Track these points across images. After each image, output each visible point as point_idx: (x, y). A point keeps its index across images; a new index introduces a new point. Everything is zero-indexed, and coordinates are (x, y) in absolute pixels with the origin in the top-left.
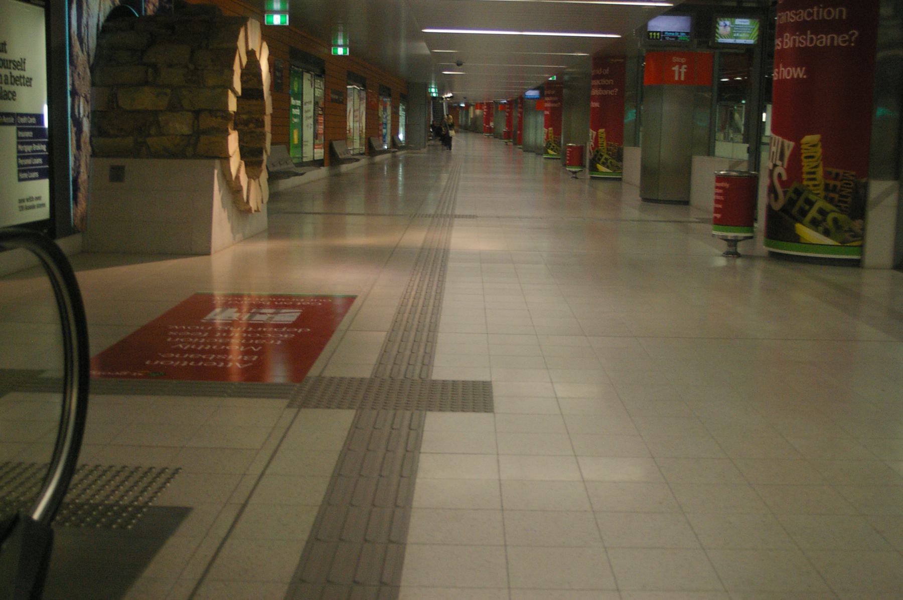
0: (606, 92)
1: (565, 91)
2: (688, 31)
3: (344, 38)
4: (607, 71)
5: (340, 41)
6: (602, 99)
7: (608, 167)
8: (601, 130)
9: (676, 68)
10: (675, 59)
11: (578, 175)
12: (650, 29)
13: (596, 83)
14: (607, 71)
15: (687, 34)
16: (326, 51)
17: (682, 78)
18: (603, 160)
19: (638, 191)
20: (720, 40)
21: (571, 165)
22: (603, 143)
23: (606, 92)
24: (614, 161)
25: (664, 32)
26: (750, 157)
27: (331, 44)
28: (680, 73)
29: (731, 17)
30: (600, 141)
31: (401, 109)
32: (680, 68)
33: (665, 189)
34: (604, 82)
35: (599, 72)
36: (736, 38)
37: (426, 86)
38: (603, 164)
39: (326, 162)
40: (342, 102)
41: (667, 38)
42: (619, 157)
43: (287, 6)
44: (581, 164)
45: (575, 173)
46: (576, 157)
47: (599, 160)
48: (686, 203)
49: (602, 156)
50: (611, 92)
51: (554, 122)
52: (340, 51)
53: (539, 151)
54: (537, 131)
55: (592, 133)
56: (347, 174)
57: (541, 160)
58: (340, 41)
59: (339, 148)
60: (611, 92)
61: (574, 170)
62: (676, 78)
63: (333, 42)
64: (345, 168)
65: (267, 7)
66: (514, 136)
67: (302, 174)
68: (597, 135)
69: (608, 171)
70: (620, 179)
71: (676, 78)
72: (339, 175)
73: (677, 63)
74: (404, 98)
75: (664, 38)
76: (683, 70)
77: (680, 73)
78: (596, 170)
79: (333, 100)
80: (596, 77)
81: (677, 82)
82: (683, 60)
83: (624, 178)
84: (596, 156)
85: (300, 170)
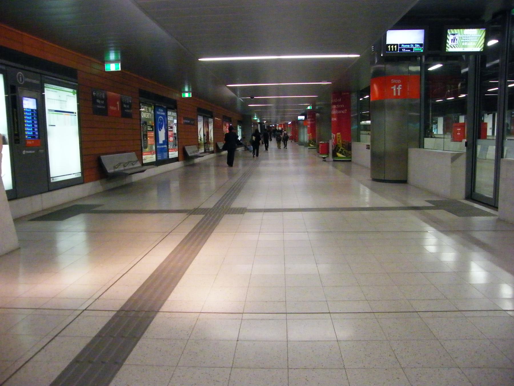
0: (340, 112)
1: (317, 115)
2: (423, 43)
3: (189, 88)
4: (340, 100)
5: (186, 89)
6: (338, 116)
7: (343, 154)
8: (339, 134)
9: (394, 88)
10: (393, 81)
11: (326, 159)
12: (388, 42)
13: (334, 107)
14: (340, 100)
15: (421, 45)
16: (178, 95)
17: (399, 94)
18: (340, 150)
19: (369, 171)
20: (450, 49)
21: (322, 154)
22: (340, 141)
23: (340, 112)
24: (346, 151)
25: (400, 45)
26: (468, 149)
27: (182, 91)
28: (397, 90)
29: (460, 28)
30: (338, 140)
31: (238, 127)
32: (397, 87)
33: (391, 171)
34: (338, 106)
35: (335, 101)
36: (464, 47)
37: (251, 116)
38: (340, 153)
39: (180, 159)
40: (193, 125)
41: (404, 50)
42: (349, 148)
43: (119, 57)
44: (327, 153)
45: (324, 158)
46: (324, 150)
47: (338, 150)
48: (404, 182)
49: (339, 148)
50: (343, 112)
51: (312, 130)
52: (187, 95)
53: (306, 145)
54: (305, 136)
55: (333, 135)
56: (199, 164)
57: (307, 149)
58: (186, 89)
59: (190, 150)
60: (343, 112)
61: (324, 156)
62: (395, 94)
63: (182, 90)
64: (197, 160)
65: (106, 59)
66: (295, 138)
67: (143, 171)
68: (336, 136)
69: (343, 156)
70: (350, 161)
71: (395, 94)
72: (194, 165)
73: (394, 84)
74: (240, 122)
75: (401, 50)
76: (399, 88)
77: (397, 90)
78: (337, 156)
79: (186, 123)
80: (334, 104)
81: (397, 97)
82: (399, 81)
83: (353, 159)
84: (335, 148)
85: (145, 168)
